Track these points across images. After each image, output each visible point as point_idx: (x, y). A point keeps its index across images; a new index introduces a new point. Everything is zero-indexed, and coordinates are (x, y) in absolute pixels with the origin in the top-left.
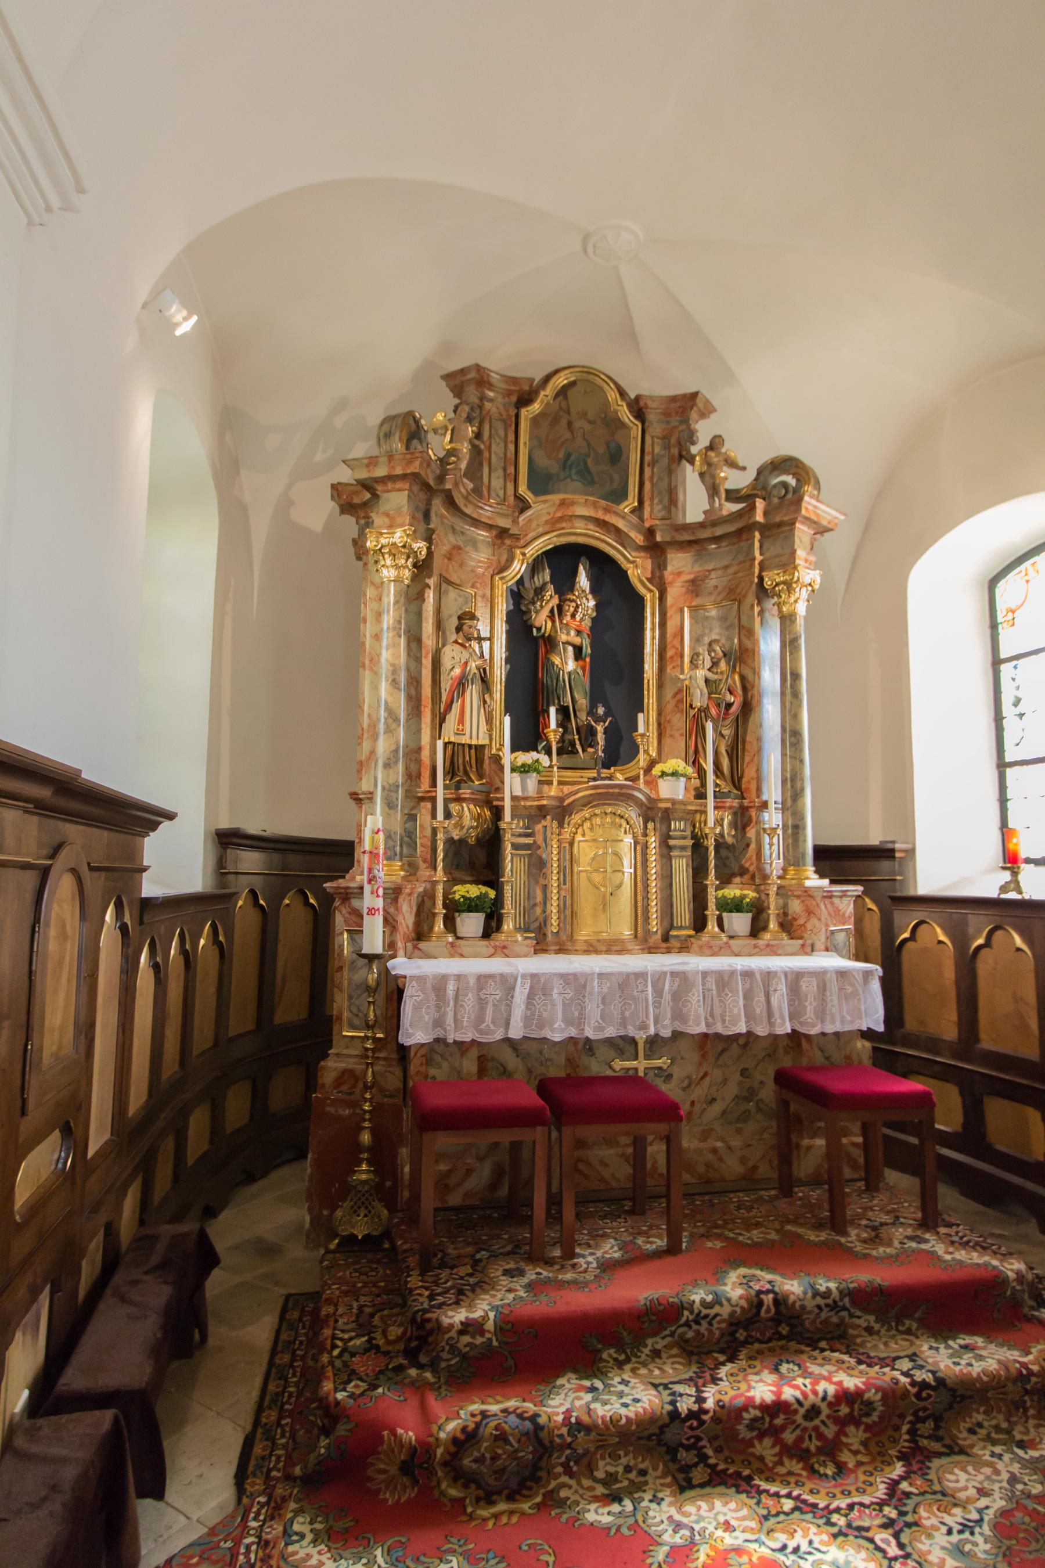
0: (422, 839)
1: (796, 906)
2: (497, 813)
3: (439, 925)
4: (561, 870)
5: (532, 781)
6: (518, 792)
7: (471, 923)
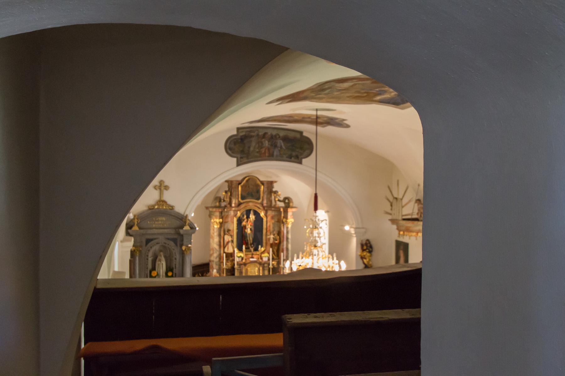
0: (222, 269)
2: (234, 264)
5: (240, 259)
6: (238, 260)
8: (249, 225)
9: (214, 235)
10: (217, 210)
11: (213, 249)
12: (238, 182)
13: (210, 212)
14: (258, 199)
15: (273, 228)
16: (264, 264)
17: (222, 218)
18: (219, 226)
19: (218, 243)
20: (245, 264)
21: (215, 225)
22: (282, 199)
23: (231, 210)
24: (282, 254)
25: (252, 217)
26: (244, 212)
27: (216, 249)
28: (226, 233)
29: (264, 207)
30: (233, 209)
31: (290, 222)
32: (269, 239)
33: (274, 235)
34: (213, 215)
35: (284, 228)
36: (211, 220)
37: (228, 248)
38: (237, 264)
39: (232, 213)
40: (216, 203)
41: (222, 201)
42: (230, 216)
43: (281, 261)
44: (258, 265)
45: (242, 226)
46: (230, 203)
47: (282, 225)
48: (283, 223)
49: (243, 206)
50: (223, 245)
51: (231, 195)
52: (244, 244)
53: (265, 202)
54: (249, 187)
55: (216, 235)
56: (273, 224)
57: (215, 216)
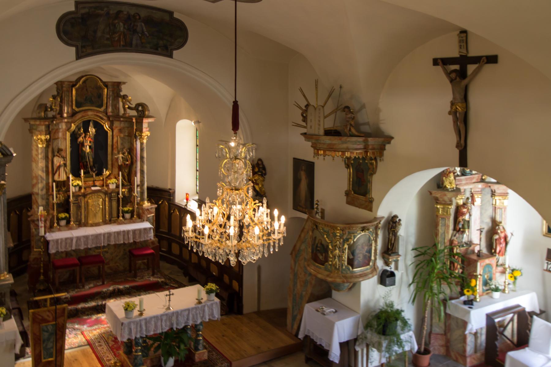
1: (141, 211)
2: (69, 196)
3: (56, 225)
4: (85, 208)
5: (77, 189)
6: (74, 191)
7: (63, 223)
8: (88, 142)
9: (39, 158)
10: (42, 123)
11: (37, 177)
12: (71, 84)
13: (31, 126)
14: (101, 106)
15: (122, 144)
16: (111, 193)
17: (49, 134)
18: (44, 146)
19: (44, 169)
20: (84, 195)
21: (40, 144)
22: (133, 106)
23: (62, 122)
24: (136, 178)
25: (92, 130)
26: (80, 123)
27: (41, 177)
28: (56, 153)
29: (108, 117)
30: (66, 120)
31: (145, 136)
32: (117, 159)
33: (123, 154)
34: (36, 129)
35: (136, 144)
36: (32, 136)
37: (59, 175)
38: (73, 196)
39: (63, 126)
40: (39, 113)
41: (49, 110)
42: (61, 130)
43: (134, 188)
44: (103, 196)
45: (78, 143)
46: (61, 113)
47: (135, 140)
48: (136, 137)
49: (79, 116)
50: (50, 170)
51: (61, 101)
52: (82, 169)
53: (110, 110)
54: (87, 90)
55: (41, 158)
56: (122, 139)
57: (39, 131)
